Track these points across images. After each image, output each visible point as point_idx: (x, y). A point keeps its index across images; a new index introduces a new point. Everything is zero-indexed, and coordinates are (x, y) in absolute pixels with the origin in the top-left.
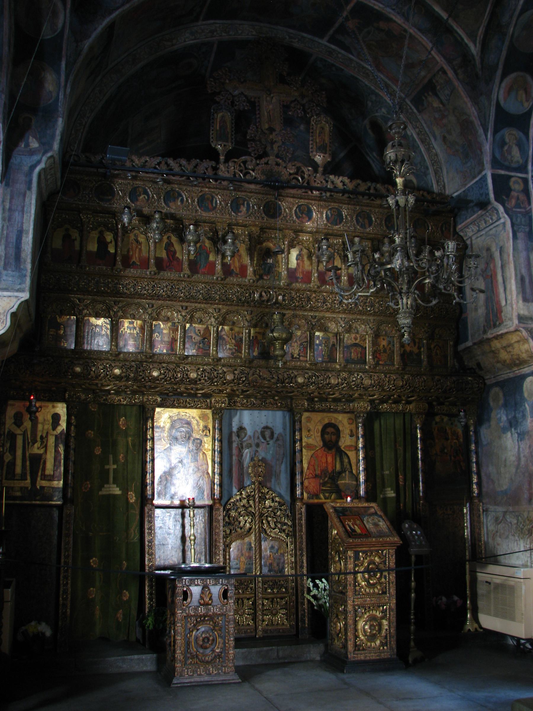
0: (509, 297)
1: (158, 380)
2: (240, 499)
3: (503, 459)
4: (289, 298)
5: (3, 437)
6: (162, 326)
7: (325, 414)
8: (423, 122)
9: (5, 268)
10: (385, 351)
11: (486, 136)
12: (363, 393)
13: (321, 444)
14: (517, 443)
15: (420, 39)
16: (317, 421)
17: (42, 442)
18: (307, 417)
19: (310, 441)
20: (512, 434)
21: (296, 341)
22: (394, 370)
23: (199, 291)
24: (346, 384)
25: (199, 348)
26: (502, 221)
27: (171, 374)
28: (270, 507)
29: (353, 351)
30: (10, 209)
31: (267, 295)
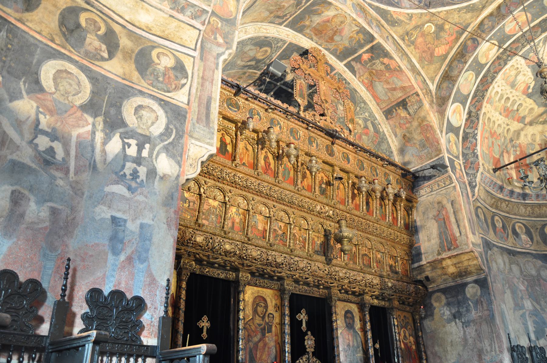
0: (463, 231)
1: (255, 260)
3: (449, 341)
6: (258, 217)
7: (345, 303)
8: (388, 126)
9: (198, 123)
11: (442, 135)
13: (345, 325)
14: (462, 329)
15: (407, 74)
20: (456, 323)
25: (281, 239)
26: (453, 185)
27: (264, 256)
30: (203, 78)
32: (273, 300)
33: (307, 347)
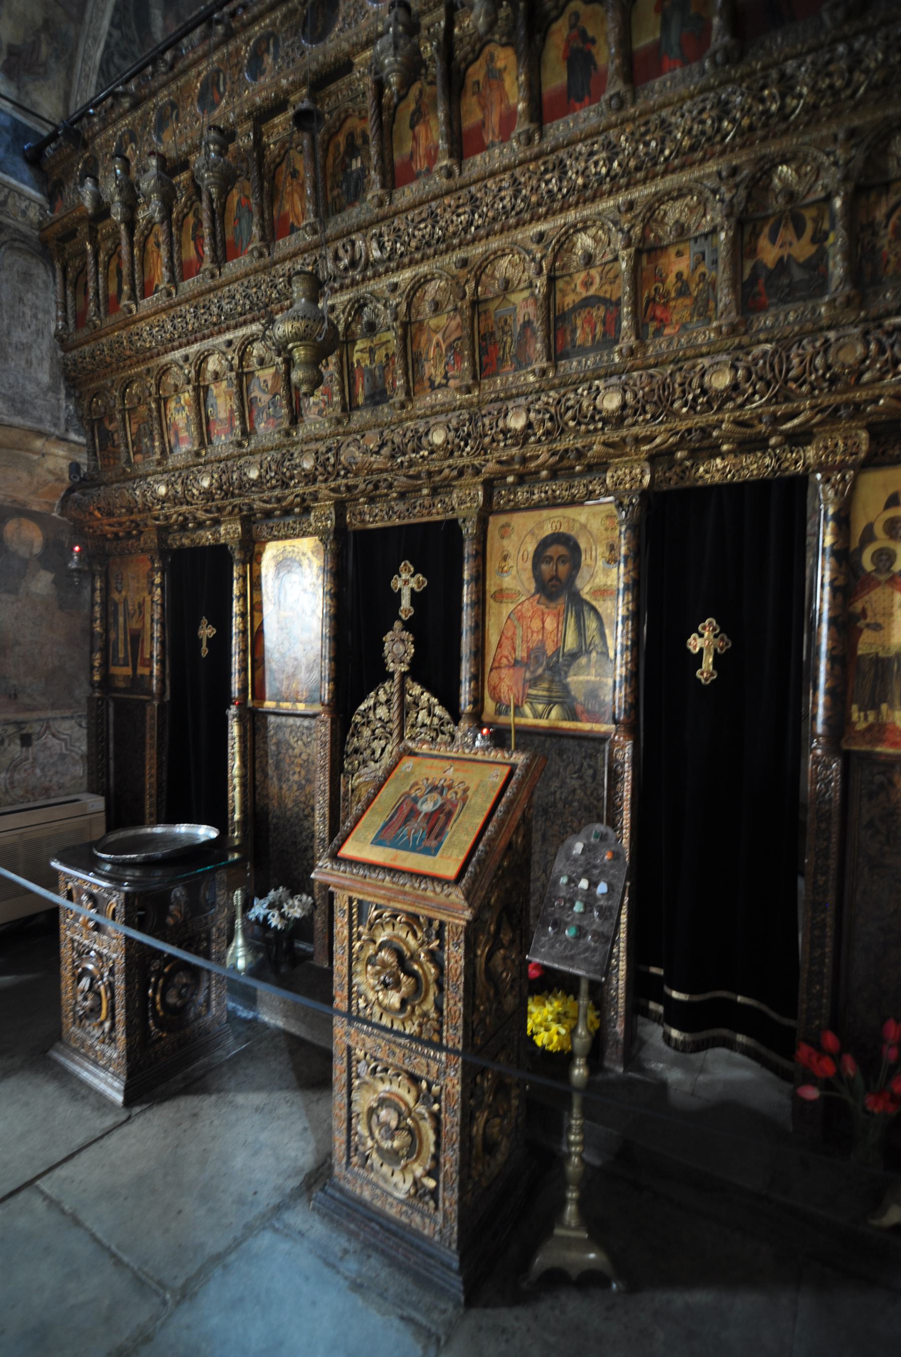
2: (375, 704)
4: (392, 237)
5: (97, 608)
7: (545, 513)
10: (683, 292)
12: (615, 437)
13: (532, 586)
16: (524, 533)
17: (141, 612)
18: (503, 526)
19: (508, 582)
21: (438, 345)
22: (710, 343)
23: (234, 298)
24: (551, 419)
25: (268, 415)
27: (224, 478)
28: (424, 725)
29: (579, 322)
31: (347, 251)
32: (314, 559)
33: (389, 660)
